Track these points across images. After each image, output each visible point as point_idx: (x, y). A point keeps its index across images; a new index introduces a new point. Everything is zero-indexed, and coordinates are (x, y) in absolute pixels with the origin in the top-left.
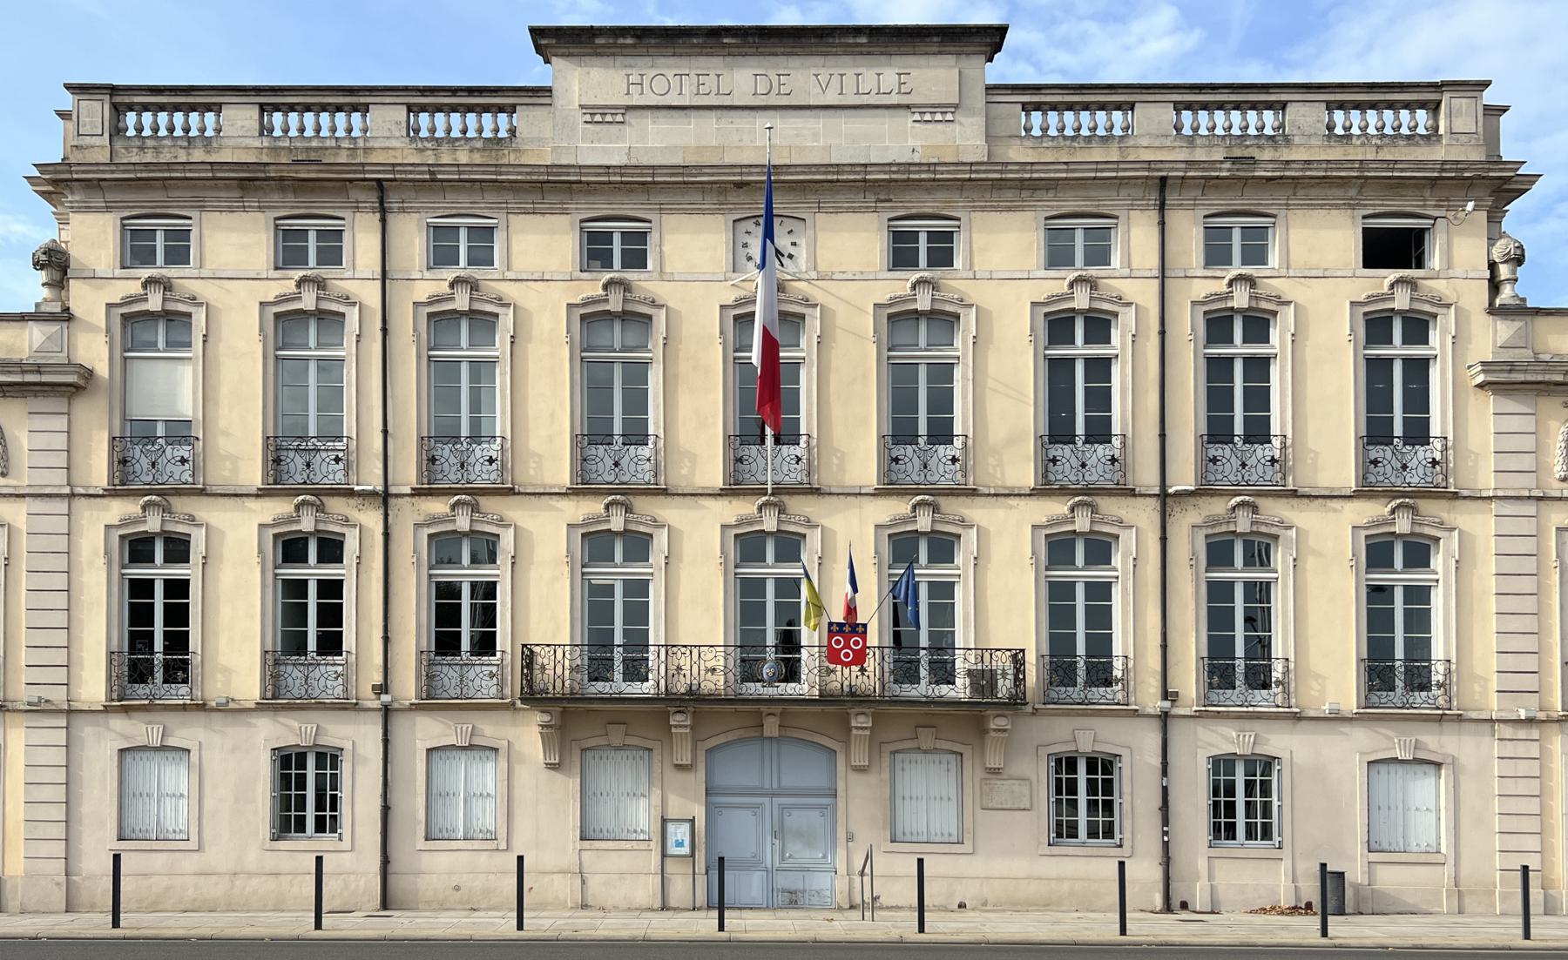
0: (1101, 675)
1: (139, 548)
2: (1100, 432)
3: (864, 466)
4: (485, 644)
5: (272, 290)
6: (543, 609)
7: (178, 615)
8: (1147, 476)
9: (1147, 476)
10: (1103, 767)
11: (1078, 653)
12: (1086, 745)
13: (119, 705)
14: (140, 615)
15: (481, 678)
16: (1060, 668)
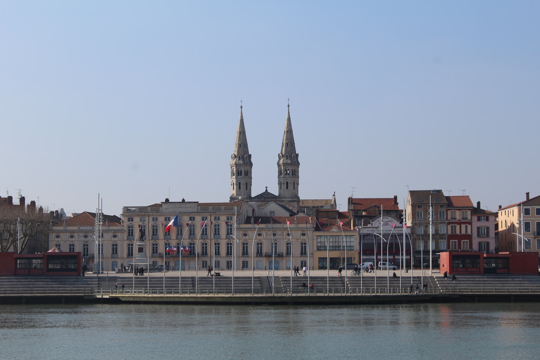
0: (206, 254)
1: (129, 245)
2: (206, 234)
3: (187, 237)
4: (157, 252)
5: (139, 224)
6: (161, 249)
7: (132, 250)
8: (209, 237)
9: (209, 237)
10: (206, 262)
11: (204, 253)
12: (204, 260)
13: (128, 257)
14: (129, 250)
15: (156, 255)
16: (203, 254)
